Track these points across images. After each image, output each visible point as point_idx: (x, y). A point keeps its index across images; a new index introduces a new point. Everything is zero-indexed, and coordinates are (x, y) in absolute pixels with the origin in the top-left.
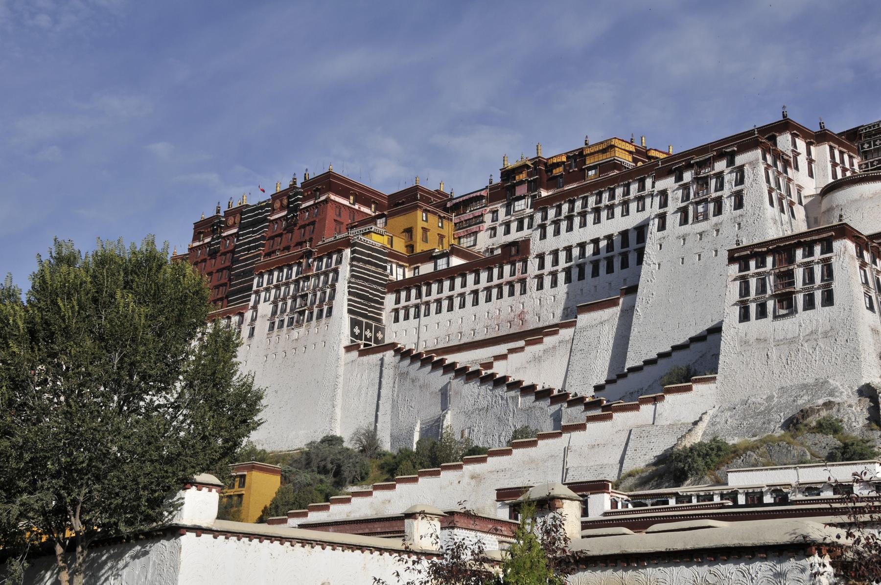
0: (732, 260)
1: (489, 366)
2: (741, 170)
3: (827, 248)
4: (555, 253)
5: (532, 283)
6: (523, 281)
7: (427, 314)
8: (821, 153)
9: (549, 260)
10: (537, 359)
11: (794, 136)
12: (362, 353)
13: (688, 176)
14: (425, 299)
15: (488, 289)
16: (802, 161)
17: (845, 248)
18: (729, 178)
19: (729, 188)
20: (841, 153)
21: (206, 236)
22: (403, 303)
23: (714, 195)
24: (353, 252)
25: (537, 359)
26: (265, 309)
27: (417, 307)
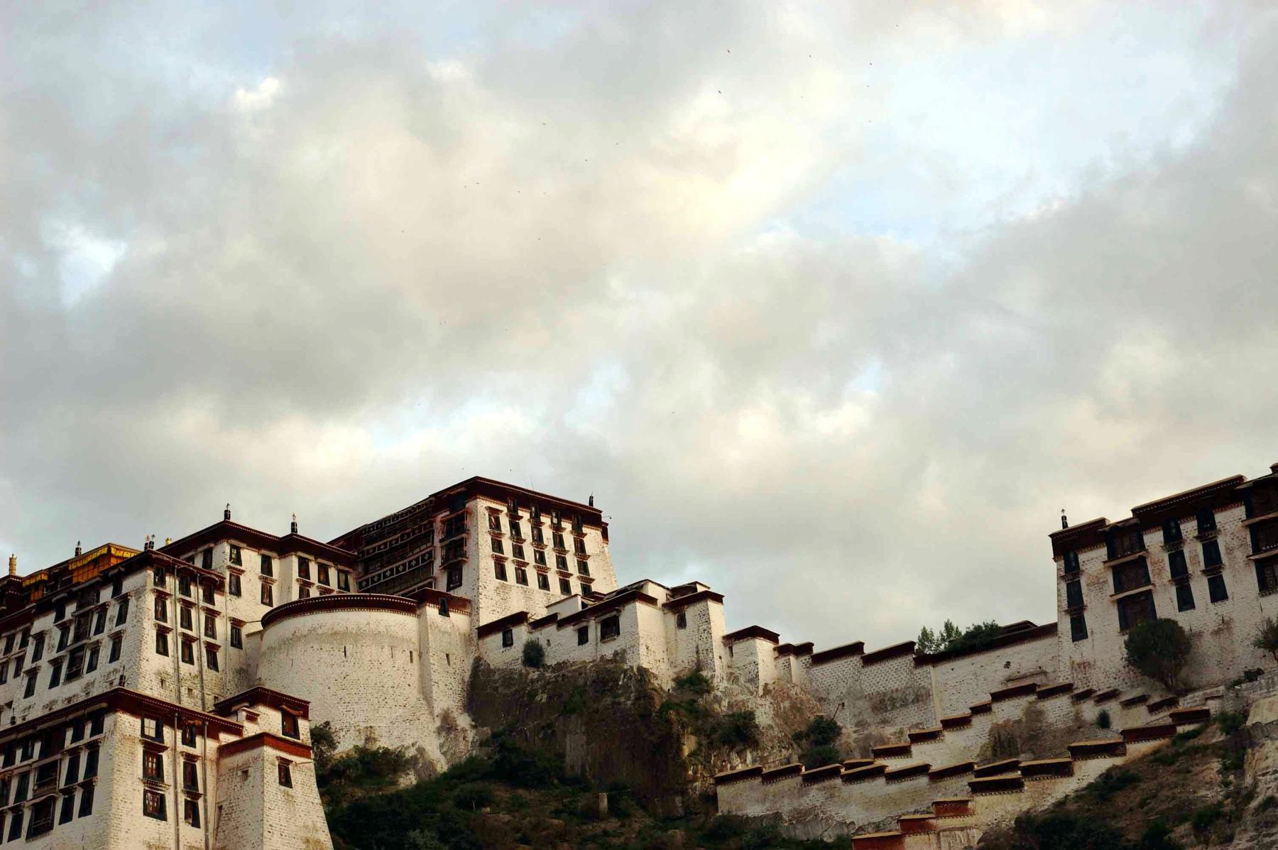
2: (124, 601)
3: (98, 729)
8: (286, 569)
17: (126, 727)
18: (113, 611)
19: (110, 627)
20: (323, 570)
23: (94, 638)
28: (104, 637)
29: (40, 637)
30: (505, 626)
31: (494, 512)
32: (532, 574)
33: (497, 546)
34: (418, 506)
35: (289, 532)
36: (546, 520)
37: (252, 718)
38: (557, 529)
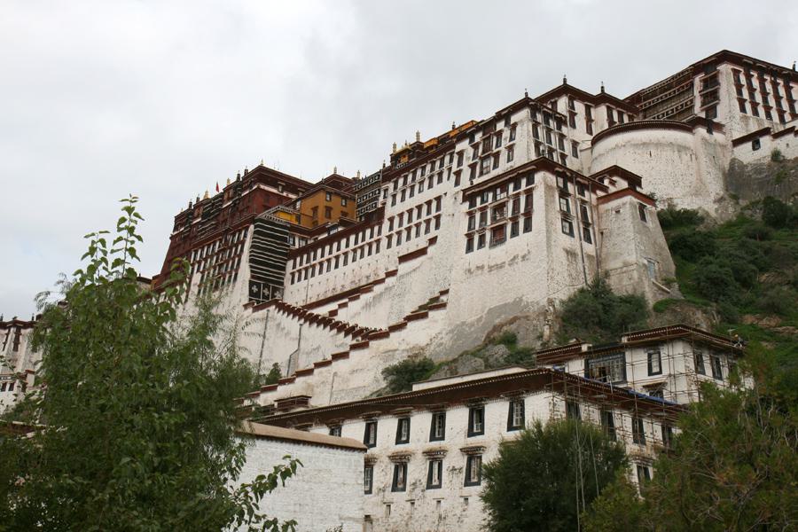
0: (464, 200)
1: (334, 313)
2: (514, 127)
4: (401, 215)
5: (384, 242)
6: (378, 241)
7: (313, 275)
8: (600, 113)
9: (396, 221)
10: (367, 306)
11: (571, 100)
12: (256, 309)
13: (478, 137)
14: (313, 263)
15: (355, 251)
16: (580, 120)
18: (506, 134)
19: (505, 143)
21: (181, 227)
22: (298, 267)
23: (495, 151)
24: (255, 227)
25: (367, 306)
26: (197, 278)
27: (306, 269)
28: (502, 148)
29: (461, 154)
30: (754, 139)
31: (736, 72)
32: (761, 111)
33: (739, 92)
34: (687, 70)
35: (599, 92)
36: (767, 77)
37: (613, 183)
38: (775, 85)
